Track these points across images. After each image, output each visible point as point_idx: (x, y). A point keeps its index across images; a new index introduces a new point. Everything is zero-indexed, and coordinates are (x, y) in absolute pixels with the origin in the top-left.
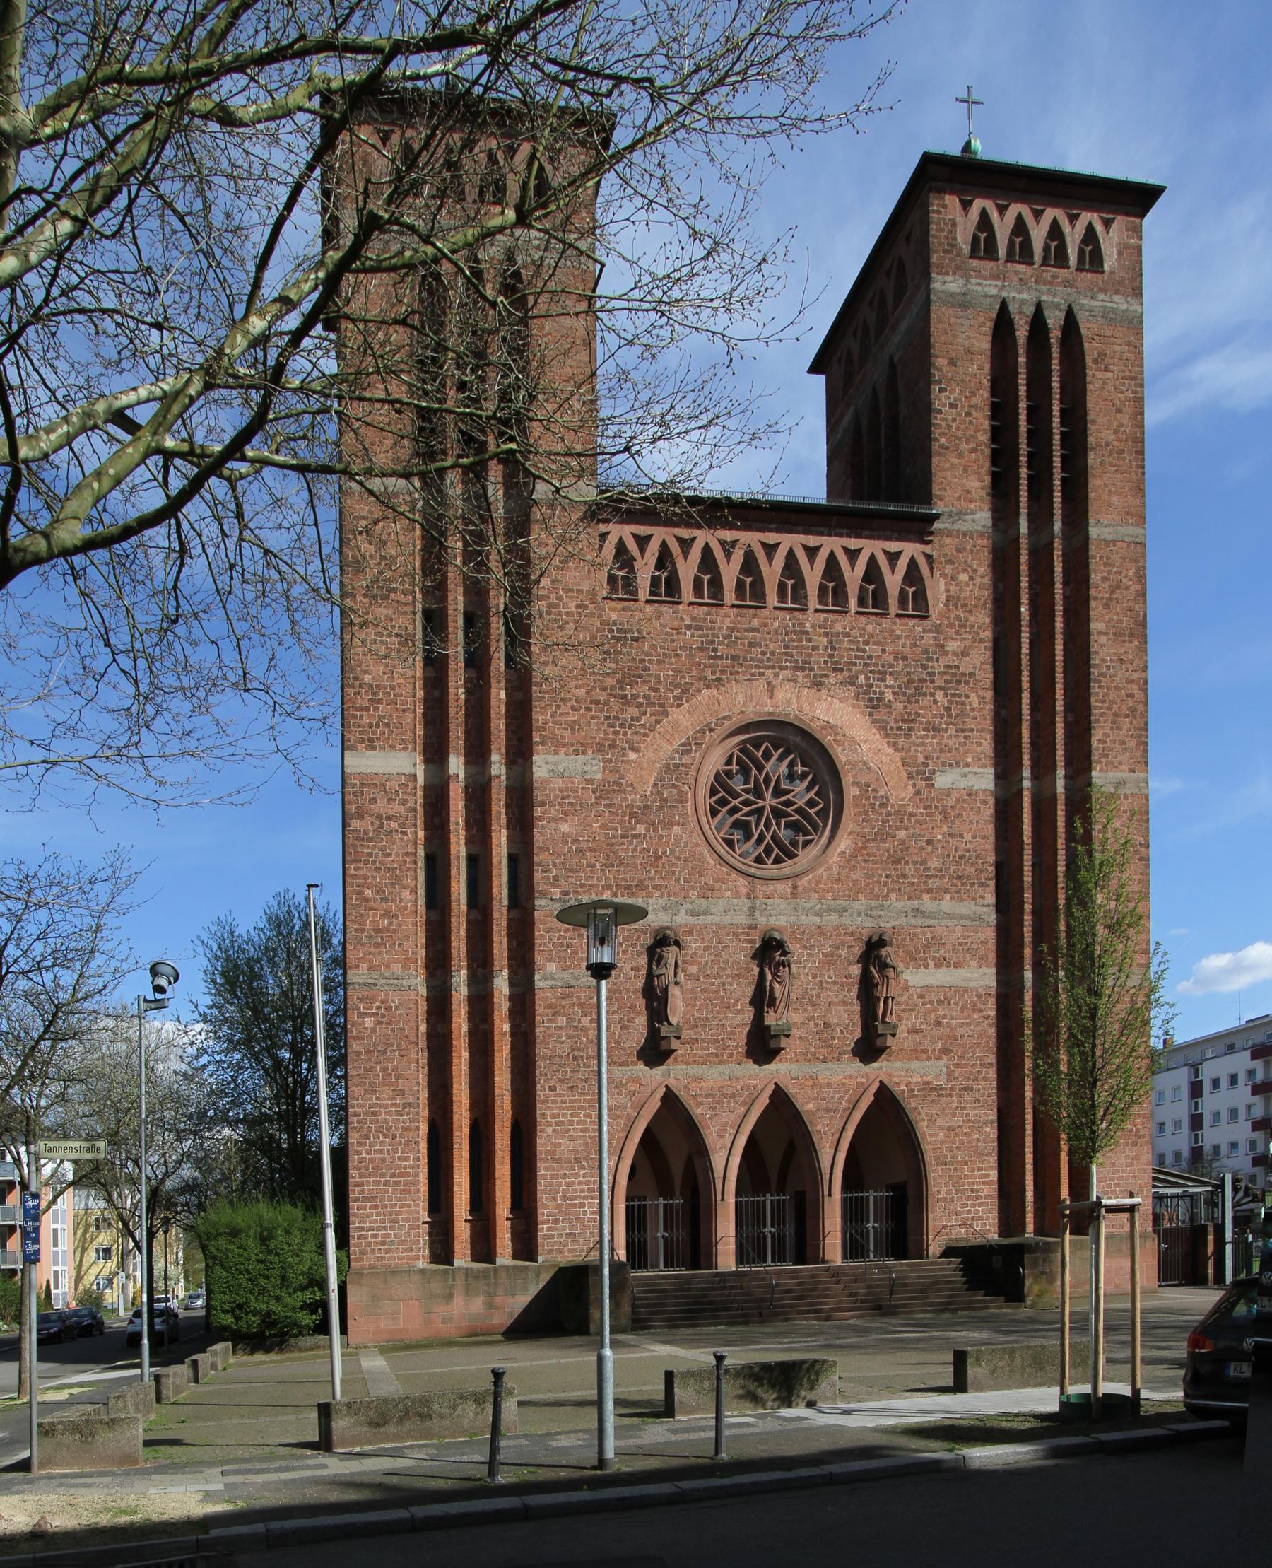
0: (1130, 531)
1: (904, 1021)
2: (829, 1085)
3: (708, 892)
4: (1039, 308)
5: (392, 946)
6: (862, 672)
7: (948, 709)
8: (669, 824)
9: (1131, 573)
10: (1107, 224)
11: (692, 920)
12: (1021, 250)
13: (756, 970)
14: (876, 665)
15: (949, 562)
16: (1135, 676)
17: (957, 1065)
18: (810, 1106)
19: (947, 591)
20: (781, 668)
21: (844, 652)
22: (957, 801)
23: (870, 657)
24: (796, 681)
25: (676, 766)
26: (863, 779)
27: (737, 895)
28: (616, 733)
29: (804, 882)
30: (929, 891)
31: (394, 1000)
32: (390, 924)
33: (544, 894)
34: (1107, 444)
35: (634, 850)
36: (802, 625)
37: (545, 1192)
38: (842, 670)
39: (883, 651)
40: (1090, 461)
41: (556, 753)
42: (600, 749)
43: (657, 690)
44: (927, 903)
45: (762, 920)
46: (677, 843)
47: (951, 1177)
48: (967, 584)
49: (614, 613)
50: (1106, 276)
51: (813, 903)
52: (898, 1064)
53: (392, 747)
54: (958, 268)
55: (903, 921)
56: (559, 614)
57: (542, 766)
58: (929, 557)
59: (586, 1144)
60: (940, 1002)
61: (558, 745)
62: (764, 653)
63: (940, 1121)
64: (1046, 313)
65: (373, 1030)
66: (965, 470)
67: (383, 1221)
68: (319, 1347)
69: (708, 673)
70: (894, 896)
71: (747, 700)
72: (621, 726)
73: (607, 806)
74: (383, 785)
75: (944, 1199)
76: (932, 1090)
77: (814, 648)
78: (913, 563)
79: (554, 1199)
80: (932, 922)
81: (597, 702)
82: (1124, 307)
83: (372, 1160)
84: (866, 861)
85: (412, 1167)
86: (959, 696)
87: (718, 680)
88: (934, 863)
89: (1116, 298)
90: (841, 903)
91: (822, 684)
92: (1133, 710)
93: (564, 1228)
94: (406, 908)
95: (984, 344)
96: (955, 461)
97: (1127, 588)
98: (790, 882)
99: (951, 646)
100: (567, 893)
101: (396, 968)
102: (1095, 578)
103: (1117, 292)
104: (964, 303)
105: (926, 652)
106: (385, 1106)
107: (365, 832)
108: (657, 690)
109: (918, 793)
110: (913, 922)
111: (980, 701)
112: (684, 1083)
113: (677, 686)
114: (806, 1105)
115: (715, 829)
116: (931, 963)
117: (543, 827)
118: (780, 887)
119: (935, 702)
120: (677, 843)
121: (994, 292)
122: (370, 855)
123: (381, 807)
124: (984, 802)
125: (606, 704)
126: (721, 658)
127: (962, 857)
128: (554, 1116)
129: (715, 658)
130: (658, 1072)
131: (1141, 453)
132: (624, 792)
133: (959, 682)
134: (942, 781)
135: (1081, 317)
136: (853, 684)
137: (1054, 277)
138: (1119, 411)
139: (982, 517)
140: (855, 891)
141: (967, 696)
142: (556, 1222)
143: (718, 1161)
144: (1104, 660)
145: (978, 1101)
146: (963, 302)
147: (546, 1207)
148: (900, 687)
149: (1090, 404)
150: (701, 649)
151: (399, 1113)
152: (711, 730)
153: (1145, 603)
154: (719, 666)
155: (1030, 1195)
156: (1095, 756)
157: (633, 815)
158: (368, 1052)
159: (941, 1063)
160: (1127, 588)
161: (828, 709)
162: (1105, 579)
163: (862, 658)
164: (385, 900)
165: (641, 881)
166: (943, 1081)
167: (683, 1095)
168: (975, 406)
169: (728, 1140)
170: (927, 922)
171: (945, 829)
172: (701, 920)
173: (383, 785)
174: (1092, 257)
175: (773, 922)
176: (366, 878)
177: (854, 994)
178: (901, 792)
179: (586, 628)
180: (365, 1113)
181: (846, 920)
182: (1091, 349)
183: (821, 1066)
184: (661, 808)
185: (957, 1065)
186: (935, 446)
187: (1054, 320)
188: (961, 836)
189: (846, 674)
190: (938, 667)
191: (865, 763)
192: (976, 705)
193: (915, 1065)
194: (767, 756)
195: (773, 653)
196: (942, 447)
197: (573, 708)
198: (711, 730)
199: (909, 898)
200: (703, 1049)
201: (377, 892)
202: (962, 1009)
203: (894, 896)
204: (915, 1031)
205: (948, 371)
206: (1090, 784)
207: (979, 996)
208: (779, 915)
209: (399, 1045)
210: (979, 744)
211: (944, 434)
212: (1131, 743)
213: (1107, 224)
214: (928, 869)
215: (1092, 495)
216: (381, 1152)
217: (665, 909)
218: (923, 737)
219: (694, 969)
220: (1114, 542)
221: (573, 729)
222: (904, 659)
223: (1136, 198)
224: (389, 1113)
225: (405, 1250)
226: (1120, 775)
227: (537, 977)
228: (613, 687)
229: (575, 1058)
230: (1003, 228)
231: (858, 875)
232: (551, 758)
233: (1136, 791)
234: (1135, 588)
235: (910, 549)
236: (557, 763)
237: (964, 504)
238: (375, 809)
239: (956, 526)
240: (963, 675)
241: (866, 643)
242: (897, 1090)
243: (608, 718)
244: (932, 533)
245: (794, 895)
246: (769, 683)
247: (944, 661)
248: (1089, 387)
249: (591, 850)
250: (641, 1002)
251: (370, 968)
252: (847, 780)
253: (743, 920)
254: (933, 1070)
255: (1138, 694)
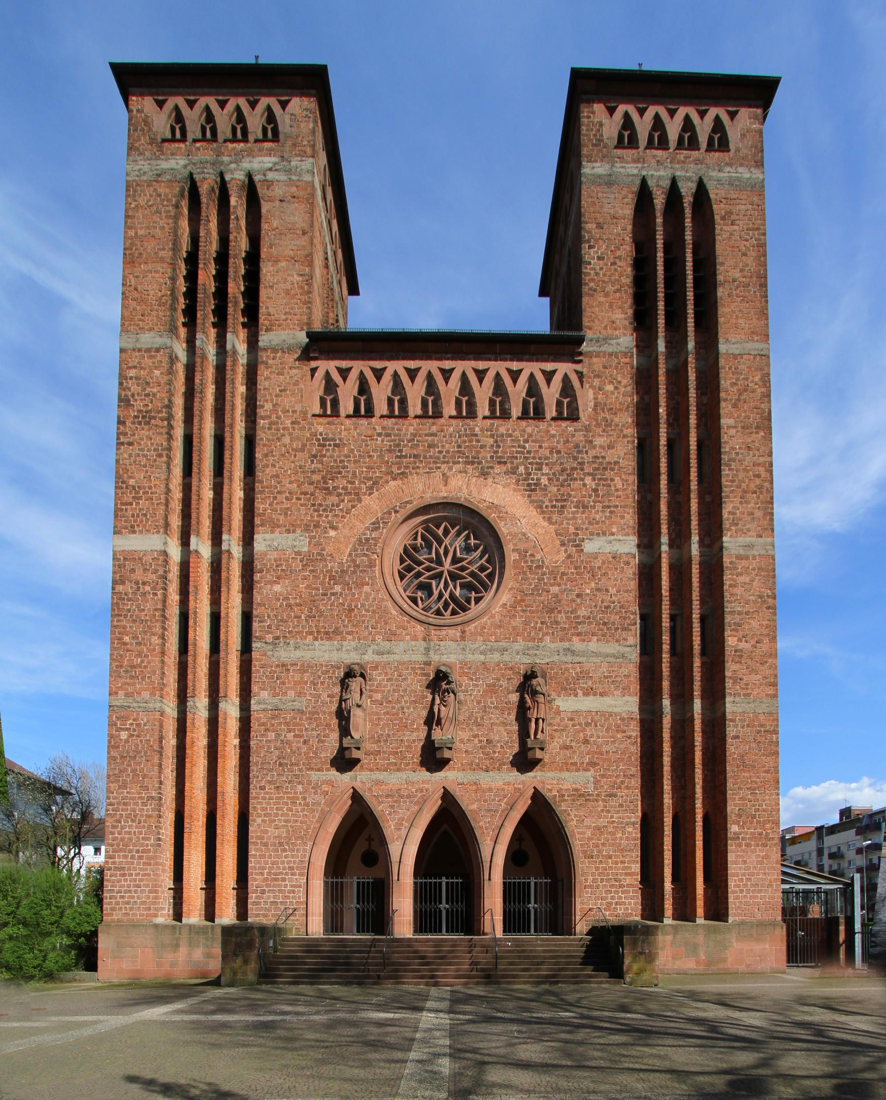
0: (754, 346)
1: (553, 744)
2: (490, 790)
3: (391, 636)
4: (674, 181)
5: (143, 679)
6: (522, 464)
7: (596, 490)
8: (361, 584)
9: (757, 379)
10: (732, 115)
11: (377, 658)
12: (658, 138)
13: (430, 697)
14: (534, 458)
15: (598, 376)
16: (761, 460)
17: (603, 776)
18: (474, 807)
19: (596, 399)
20: (454, 463)
21: (508, 448)
22: (603, 563)
23: (529, 452)
24: (466, 472)
25: (367, 540)
26: (521, 547)
27: (415, 638)
28: (320, 516)
29: (472, 627)
30: (579, 634)
31: (143, 719)
32: (142, 662)
33: (260, 638)
34: (734, 280)
35: (332, 605)
36: (472, 430)
37: (255, 868)
38: (505, 463)
39: (541, 447)
40: (719, 294)
41: (273, 532)
42: (307, 529)
43: (353, 483)
44: (577, 644)
45: (435, 658)
46: (367, 599)
47: (597, 868)
48: (612, 393)
49: (321, 427)
50: (731, 154)
51: (479, 644)
52: (550, 774)
53: (148, 531)
54: (604, 157)
55: (556, 658)
56: (278, 430)
57: (260, 543)
58: (580, 375)
59: (288, 832)
60: (588, 724)
61: (274, 526)
62: (440, 452)
63: (587, 822)
64: (680, 185)
65: (127, 741)
66: (611, 306)
67: (129, 886)
68: (75, 980)
69: (396, 471)
70: (547, 638)
71: (424, 488)
72: (324, 510)
73: (312, 571)
74: (140, 559)
75: (591, 887)
76: (580, 795)
77: (482, 447)
78: (566, 379)
79: (262, 874)
80: (580, 660)
81: (305, 494)
82: (748, 176)
83: (123, 839)
84: (524, 611)
85: (152, 845)
86: (606, 480)
87: (403, 473)
88: (582, 612)
89: (740, 170)
90: (503, 644)
91: (488, 474)
92: (760, 487)
93: (269, 897)
94: (154, 650)
95: (628, 211)
96: (602, 299)
97: (753, 391)
98: (459, 628)
99: (598, 441)
100: (278, 638)
101: (146, 695)
102: (724, 383)
103: (741, 165)
104: (611, 184)
105: (577, 446)
106: (133, 799)
107: (126, 594)
108: (353, 483)
109: (569, 556)
110: (564, 659)
111: (625, 484)
112: (368, 785)
113: (370, 479)
114: (469, 804)
115: (398, 589)
116: (580, 692)
117: (261, 588)
118: (451, 632)
119: (585, 485)
120: (367, 599)
121: (635, 172)
122: (129, 610)
123: (139, 575)
124: (628, 563)
125: (312, 494)
126: (406, 457)
127: (607, 607)
128: (263, 809)
129: (401, 457)
130: (347, 776)
131: (764, 285)
132: (325, 560)
133: (605, 469)
134: (590, 547)
135: (710, 186)
136: (514, 473)
137: (686, 158)
138: (744, 255)
139: (627, 341)
140: (515, 634)
141: (612, 480)
142: (263, 892)
143: (394, 849)
144: (733, 449)
145: (621, 805)
146: (609, 182)
147: (255, 880)
148: (554, 474)
149: (719, 248)
150: (390, 451)
151: (144, 804)
152: (396, 512)
153: (769, 402)
154: (402, 462)
155: (668, 886)
156: (726, 524)
157: (332, 578)
158: (122, 757)
159: (589, 774)
160: (753, 391)
161: (493, 493)
162: (733, 384)
163: (522, 453)
164: (139, 644)
165: (336, 628)
166: (591, 788)
167: (367, 796)
168: (620, 258)
169: (404, 832)
170: (577, 659)
171: (593, 585)
172: (385, 658)
173: (140, 559)
174: (719, 141)
175: (444, 659)
176: (125, 627)
177: (513, 717)
178: (555, 556)
179: (298, 439)
180: (119, 804)
181: (506, 657)
182: (718, 209)
183: (483, 774)
184: (354, 572)
185: (603, 776)
186: (585, 289)
187: (687, 190)
188: (607, 590)
189: (509, 466)
190: (587, 458)
191: (524, 534)
192: (619, 486)
193: (565, 775)
194: (446, 532)
195: (448, 452)
196: (591, 289)
197: (287, 498)
198: (396, 512)
199: (562, 640)
200: (384, 759)
201: (133, 638)
202: (607, 730)
203: (547, 638)
204: (566, 747)
205: (596, 233)
206: (721, 548)
207: (622, 719)
208: (449, 653)
209: (146, 752)
210: (622, 517)
211: (592, 280)
212: (759, 514)
213: (732, 115)
214: (578, 617)
215: (721, 320)
216: (129, 833)
217: (356, 649)
218: (573, 513)
219: (378, 696)
220: (741, 355)
221: (286, 514)
222: (559, 452)
223: (759, 92)
224: (136, 804)
225: (146, 909)
226: (748, 540)
227: (253, 702)
228: (319, 481)
229: (281, 765)
230: (643, 126)
231: (518, 622)
232: (268, 536)
233: (763, 552)
234: (760, 390)
235: (563, 368)
236: (273, 540)
237: (610, 331)
238: (134, 577)
239: (603, 349)
240: (610, 463)
241: (526, 441)
242: (548, 795)
243: (314, 505)
244: (581, 354)
245: (463, 638)
246: (444, 475)
247: (592, 453)
248: (717, 238)
249: (297, 605)
250: (335, 721)
251: (127, 695)
252: (508, 548)
253: (420, 658)
254: (584, 779)
255: (763, 474)
